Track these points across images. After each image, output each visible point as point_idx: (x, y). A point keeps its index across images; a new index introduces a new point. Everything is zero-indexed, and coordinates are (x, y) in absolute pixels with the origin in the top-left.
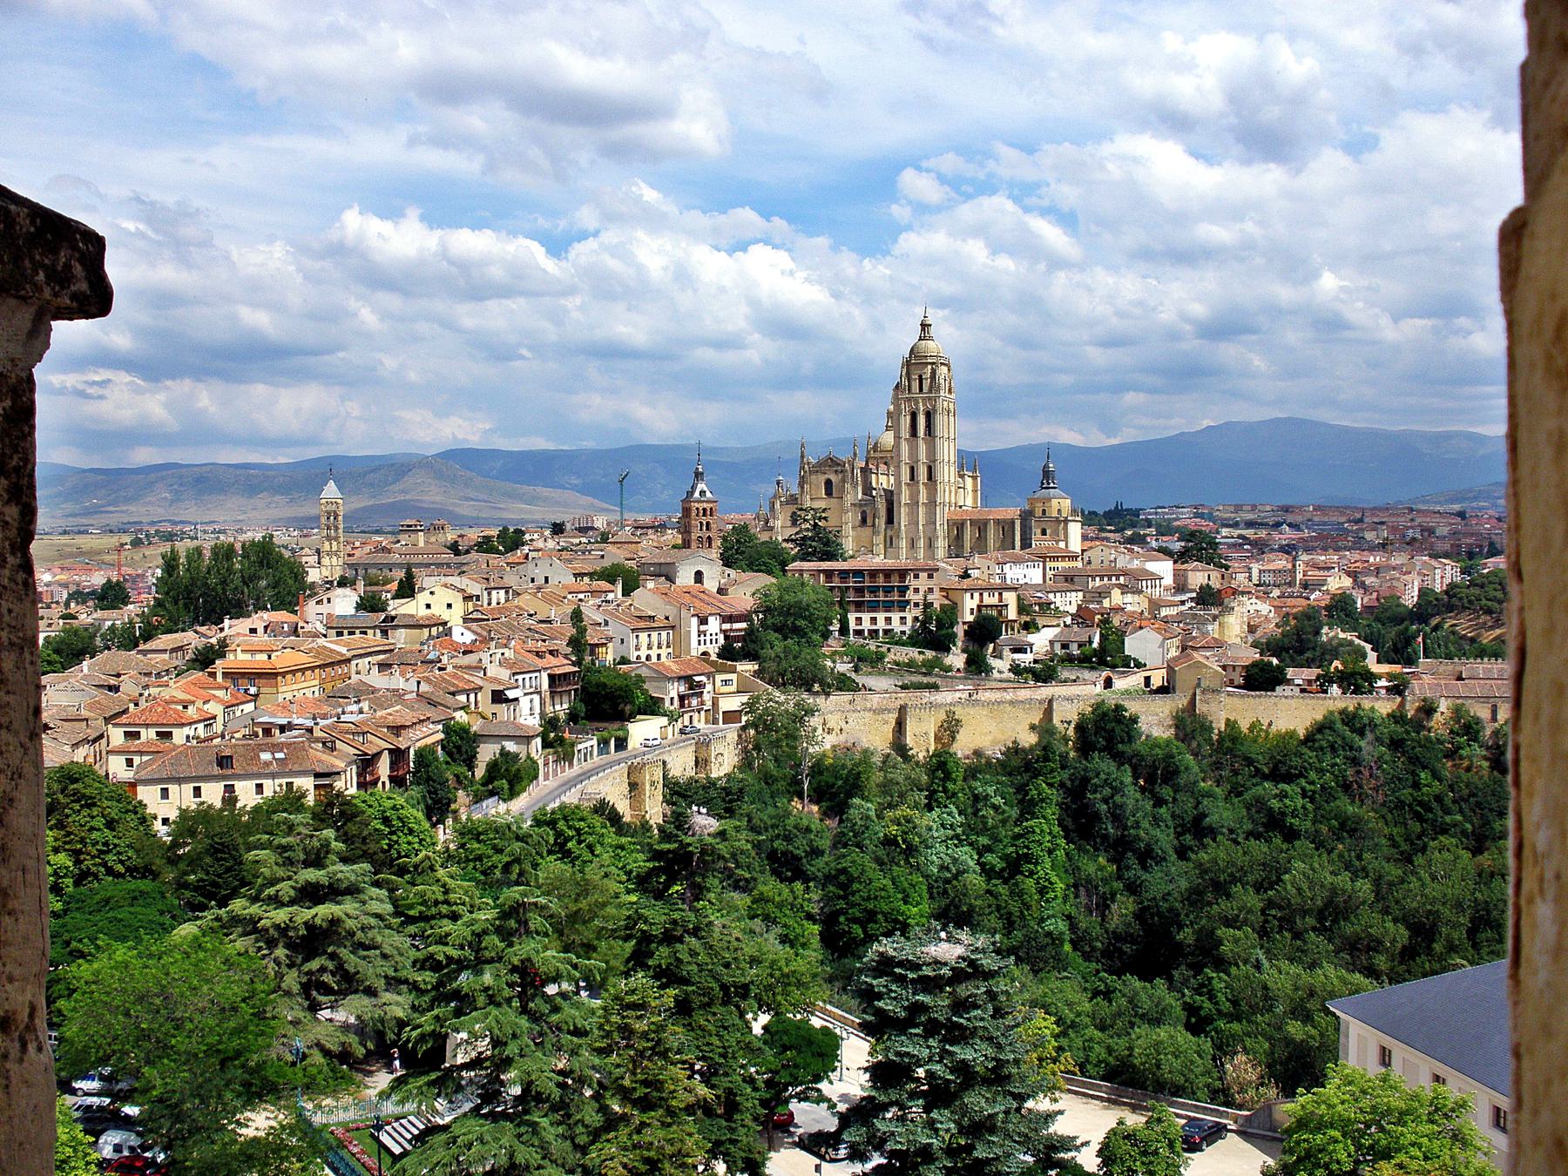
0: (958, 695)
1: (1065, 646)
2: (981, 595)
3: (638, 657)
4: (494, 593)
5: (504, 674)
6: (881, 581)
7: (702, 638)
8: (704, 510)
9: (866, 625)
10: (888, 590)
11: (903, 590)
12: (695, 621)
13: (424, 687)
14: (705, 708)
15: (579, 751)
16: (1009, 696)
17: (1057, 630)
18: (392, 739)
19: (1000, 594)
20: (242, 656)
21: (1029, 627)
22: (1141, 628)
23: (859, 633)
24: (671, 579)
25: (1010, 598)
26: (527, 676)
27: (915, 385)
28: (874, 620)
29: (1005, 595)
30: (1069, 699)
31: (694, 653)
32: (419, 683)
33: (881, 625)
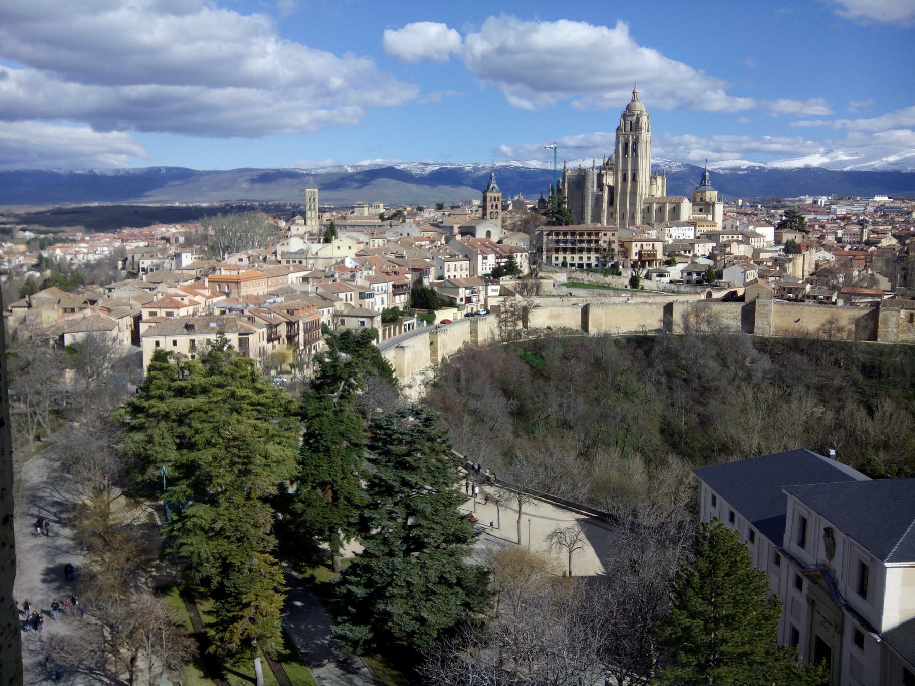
0: (621, 299)
1: (689, 274)
2: (642, 245)
3: (449, 277)
4: (376, 241)
5: (367, 284)
6: (585, 237)
7: (484, 267)
8: (495, 197)
9: (577, 261)
10: (589, 242)
11: (597, 242)
12: (480, 257)
13: (320, 290)
14: (480, 303)
15: (405, 325)
16: (650, 300)
17: (686, 265)
18: (289, 316)
19: (653, 245)
20: (224, 273)
21: (669, 263)
22: (733, 264)
23: (573, 265)
24: (473, 235)
25: (659, 246)
26: (380, 285)
27: (628, 127)
28: (581, 258)
29: (656, 244)
30: (683, 303)
31: (480, 275)
32: (317, 288)
33: (585, 261)
